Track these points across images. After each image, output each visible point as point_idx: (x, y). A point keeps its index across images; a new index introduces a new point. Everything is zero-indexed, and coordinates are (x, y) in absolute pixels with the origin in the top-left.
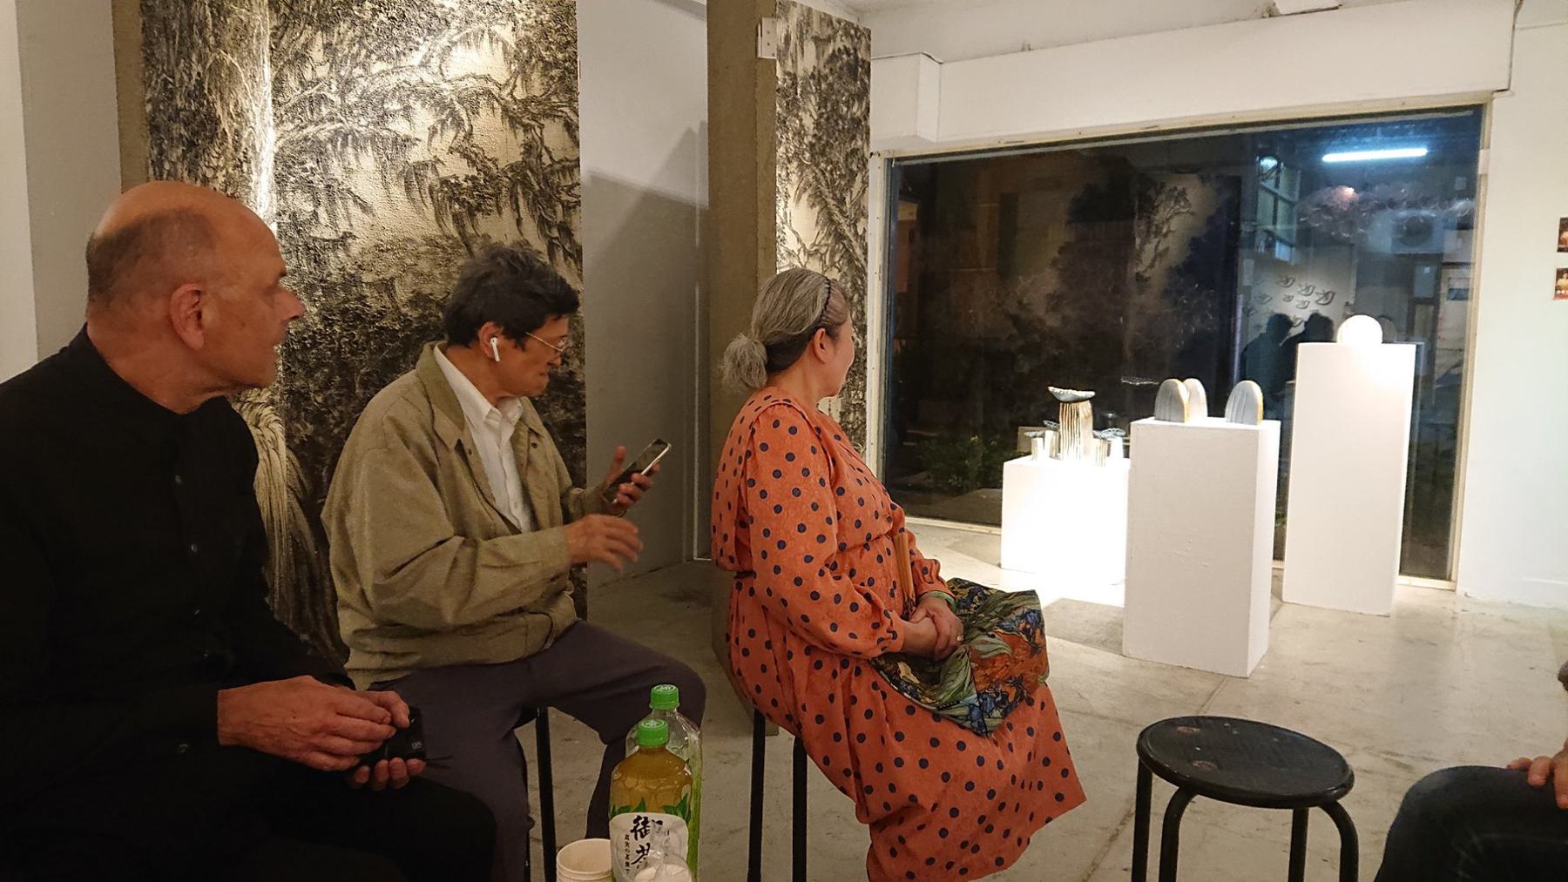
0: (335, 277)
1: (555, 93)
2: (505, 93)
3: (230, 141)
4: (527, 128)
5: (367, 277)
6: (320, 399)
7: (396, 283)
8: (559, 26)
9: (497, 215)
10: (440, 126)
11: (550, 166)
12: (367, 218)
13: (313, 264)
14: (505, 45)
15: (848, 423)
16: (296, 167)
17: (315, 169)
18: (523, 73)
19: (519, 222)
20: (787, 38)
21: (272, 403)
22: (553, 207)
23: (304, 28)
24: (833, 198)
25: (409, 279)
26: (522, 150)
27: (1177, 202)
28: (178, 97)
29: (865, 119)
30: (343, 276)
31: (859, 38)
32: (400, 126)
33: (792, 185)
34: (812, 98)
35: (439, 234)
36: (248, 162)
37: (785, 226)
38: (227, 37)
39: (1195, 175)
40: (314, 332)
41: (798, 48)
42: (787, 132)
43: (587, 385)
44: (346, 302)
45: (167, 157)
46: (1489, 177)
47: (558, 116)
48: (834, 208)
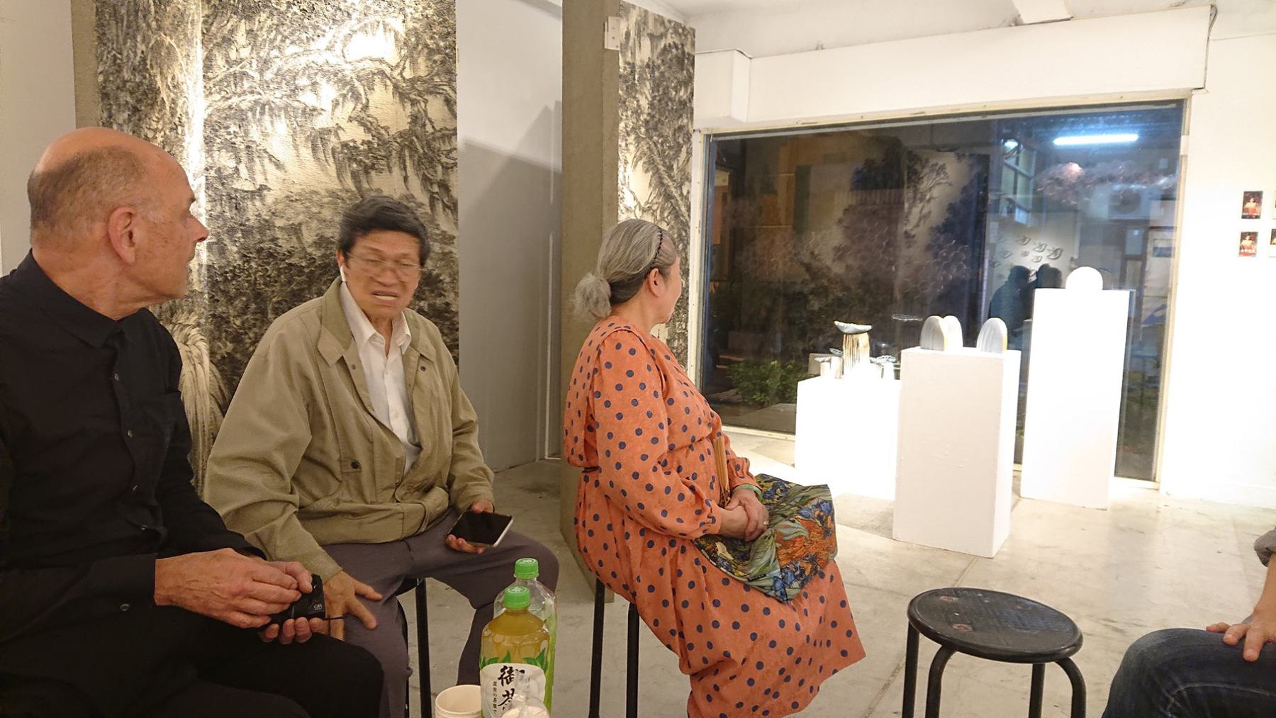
0: (253, 221)
1: (437, 74)
2: (396, 73)
3: (168, 108)
4: (414, 103)
5: (279, 223)
6: (238, 322)
7: (303, 227)
8: (441, 19)
9: (388, 173)
10: (341, 100)
11: (433, 133)
12: (279, 173)
13: (234, 211)
14: (396, 34)
16: (222, 130)
17: (238, 133)
18: (412, 58)
19: (406, 179)
20: (628, 34)
21: (198, 325)
22: (434, 167)
23: (231, 17)
24: (663, 166)
25: (314, 224)
26: (409, 120)
27: (938, 174)
28: (125, 70)
29: (690, 101)
30: (259, 221)
31: (686, 36)
32: (308, 98)
33: (631, 153)
34: (648, 83)
35: (340, 188)
36: (182, 126)
38: (167, 23)
39: (952, 154)
40: (235, 267)
41: (637, 42)
42: (627, 111)
43: (460, 315)
44: (261, 243)
45: (114, 120)
46: (1189, 158)
47: (439, 93)
48: (664, 173)
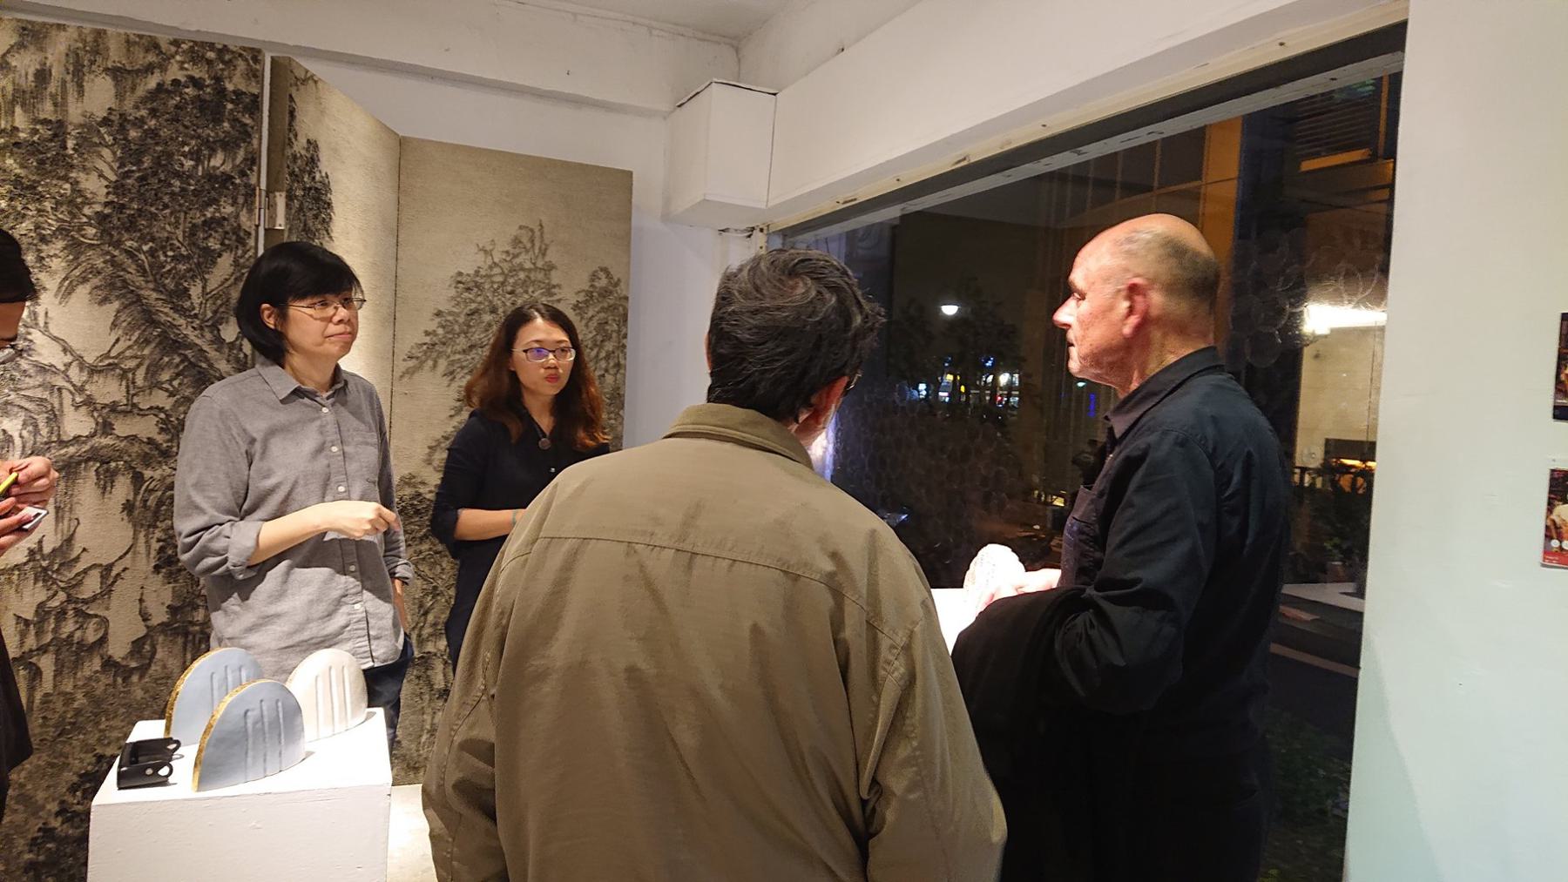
15: (192, 623)
20: (42, 76)
34: (106, 152)
37: (31, 330)
